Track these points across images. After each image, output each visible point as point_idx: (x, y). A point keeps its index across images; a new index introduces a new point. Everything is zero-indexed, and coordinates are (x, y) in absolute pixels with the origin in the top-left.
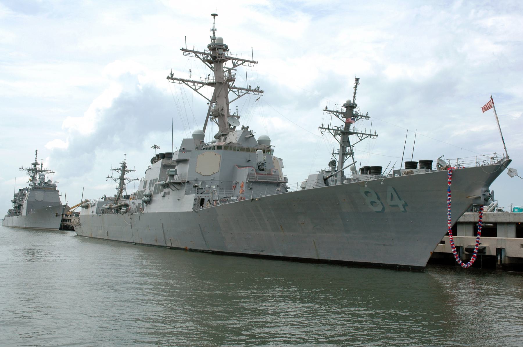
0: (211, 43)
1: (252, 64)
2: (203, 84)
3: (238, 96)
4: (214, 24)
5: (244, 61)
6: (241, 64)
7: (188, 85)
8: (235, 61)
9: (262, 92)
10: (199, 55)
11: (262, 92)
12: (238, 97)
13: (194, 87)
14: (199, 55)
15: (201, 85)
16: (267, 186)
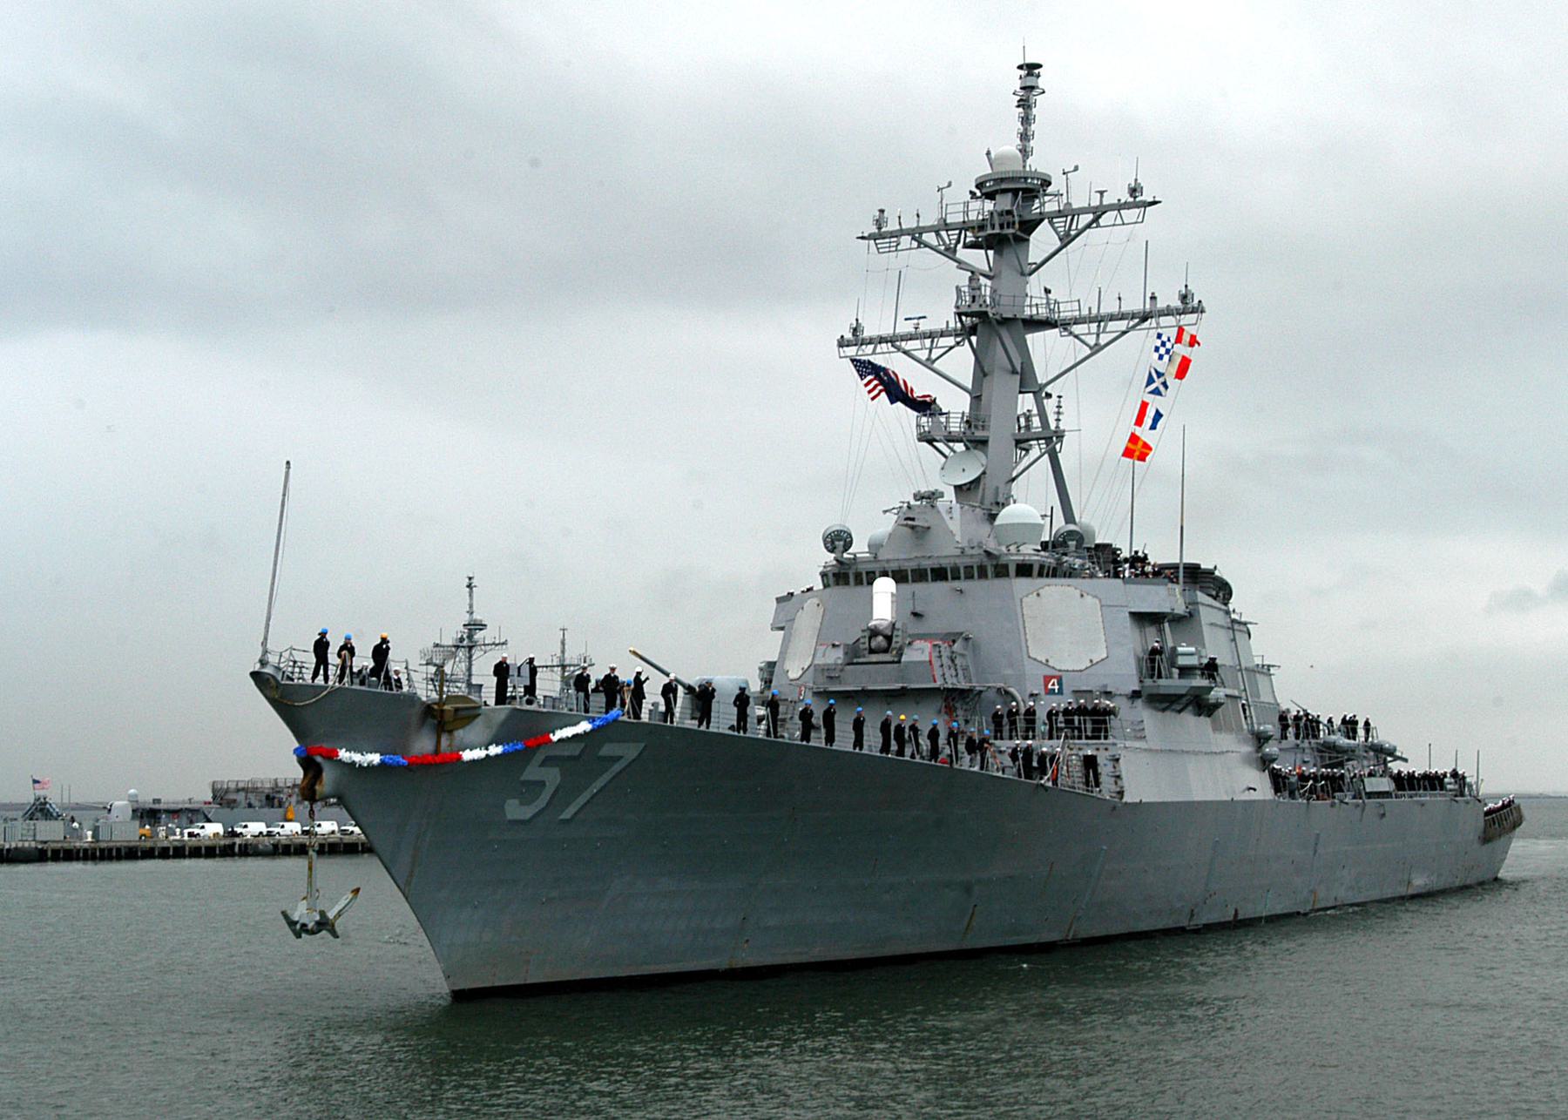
2: (957, 335)
3: (1091, 348)
5: (1098, 212)
6: (1089, 226)
8: (1064, 219)
10: (930, 238)
11: (1199, 310)
13: (923, 355)
14: (925, 237)
15: (951, 341)
16: (917, 703)
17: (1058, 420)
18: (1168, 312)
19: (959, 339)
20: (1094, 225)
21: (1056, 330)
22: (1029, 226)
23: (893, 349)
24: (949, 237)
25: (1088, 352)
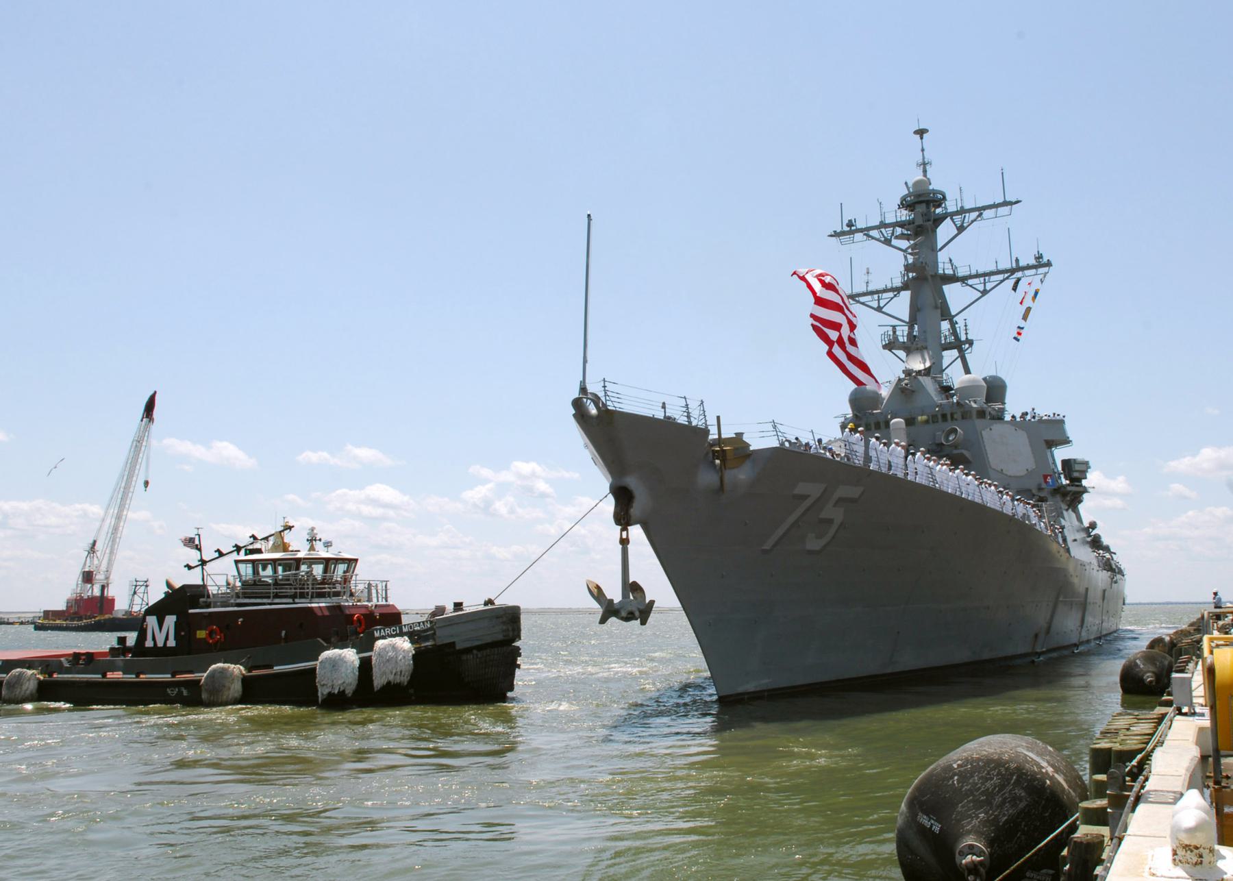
0: (907, 192)
1: (1003, 210)
4: (923, 150)
5: (980, 210)
7: (863, 304)
9: (1049, 264)
10: (874, 233)
11: (1049, 264)
12: (981, 295)
13: (875, 304)
15: (891, 294)
17: (966, 334)
18: (1029, 267)
19: (895, 293)
20: (979, 219)
21: (959, 284)
22: (939, 220)
23: (854, 302)
24: (887, 232)
25: (980, 294)
